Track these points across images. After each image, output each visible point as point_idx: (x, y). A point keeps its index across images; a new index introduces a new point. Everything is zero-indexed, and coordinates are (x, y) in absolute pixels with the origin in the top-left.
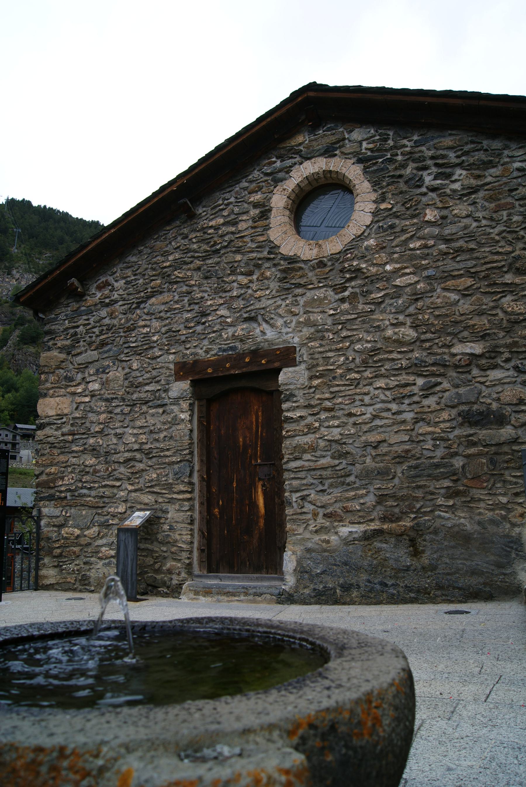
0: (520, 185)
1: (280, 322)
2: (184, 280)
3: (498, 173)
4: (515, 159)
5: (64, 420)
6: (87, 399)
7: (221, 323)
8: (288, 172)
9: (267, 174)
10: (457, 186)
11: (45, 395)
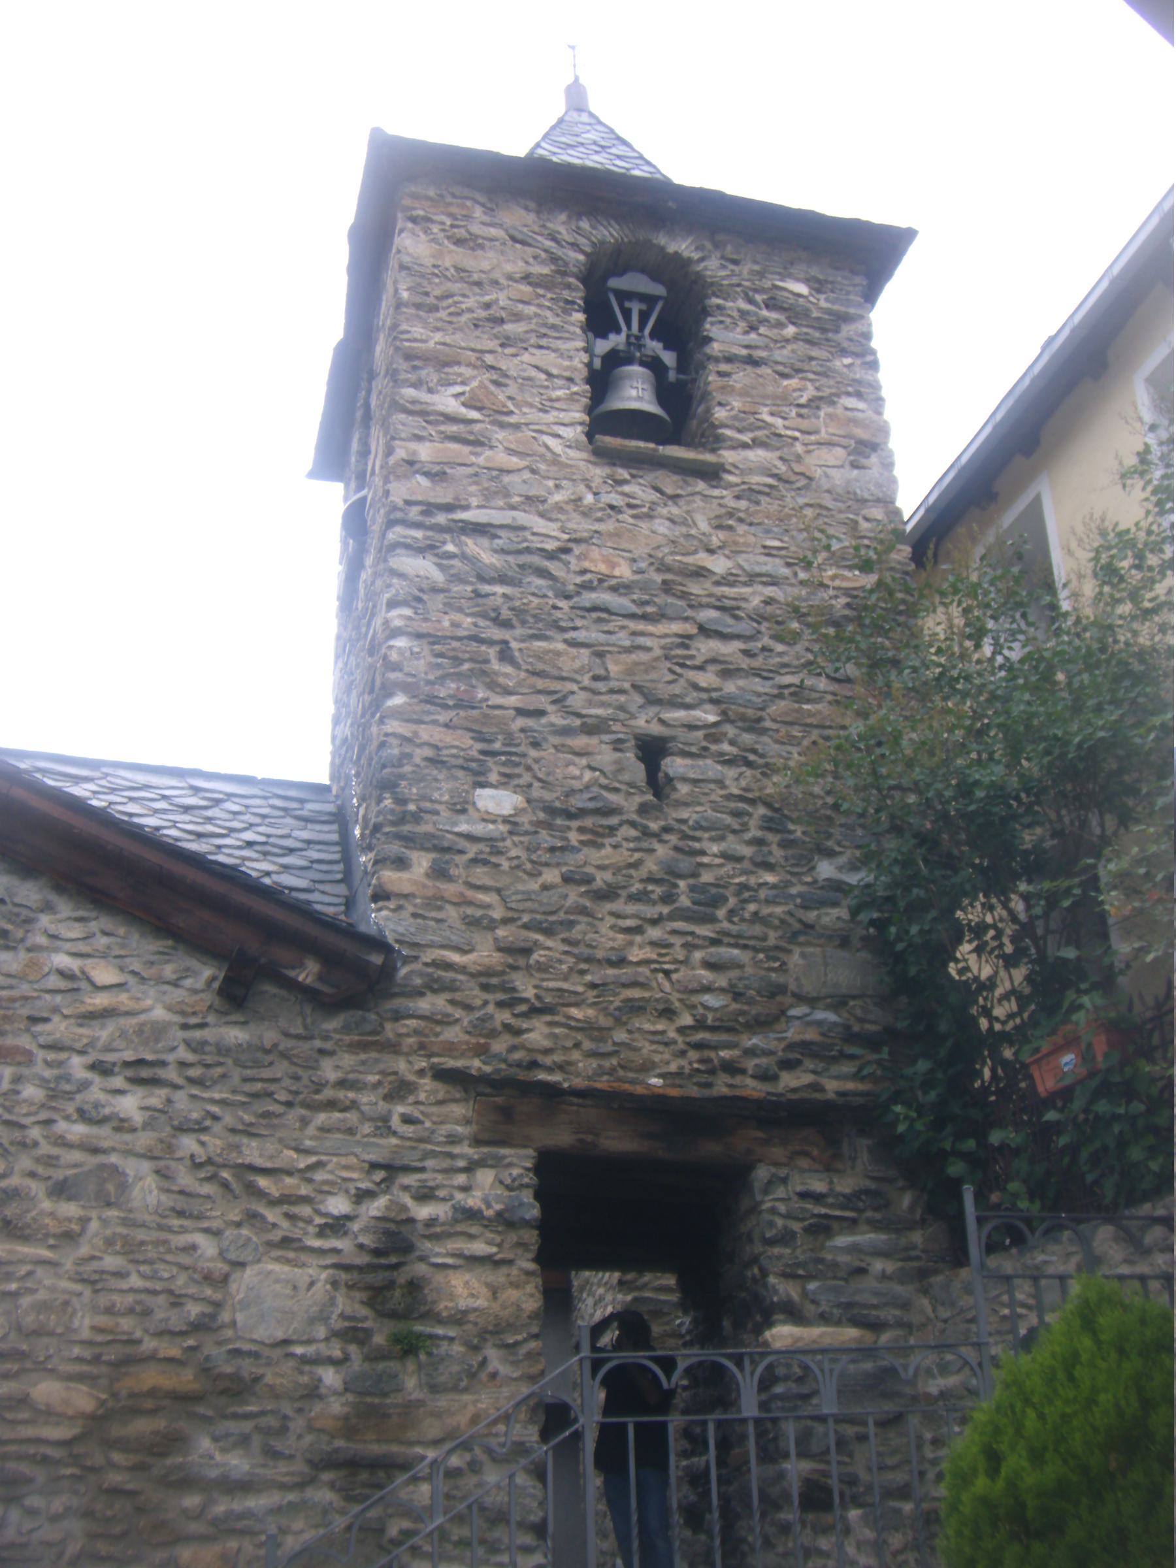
0: (56, 1010)
3: (14, 968)
4: (59, 943)
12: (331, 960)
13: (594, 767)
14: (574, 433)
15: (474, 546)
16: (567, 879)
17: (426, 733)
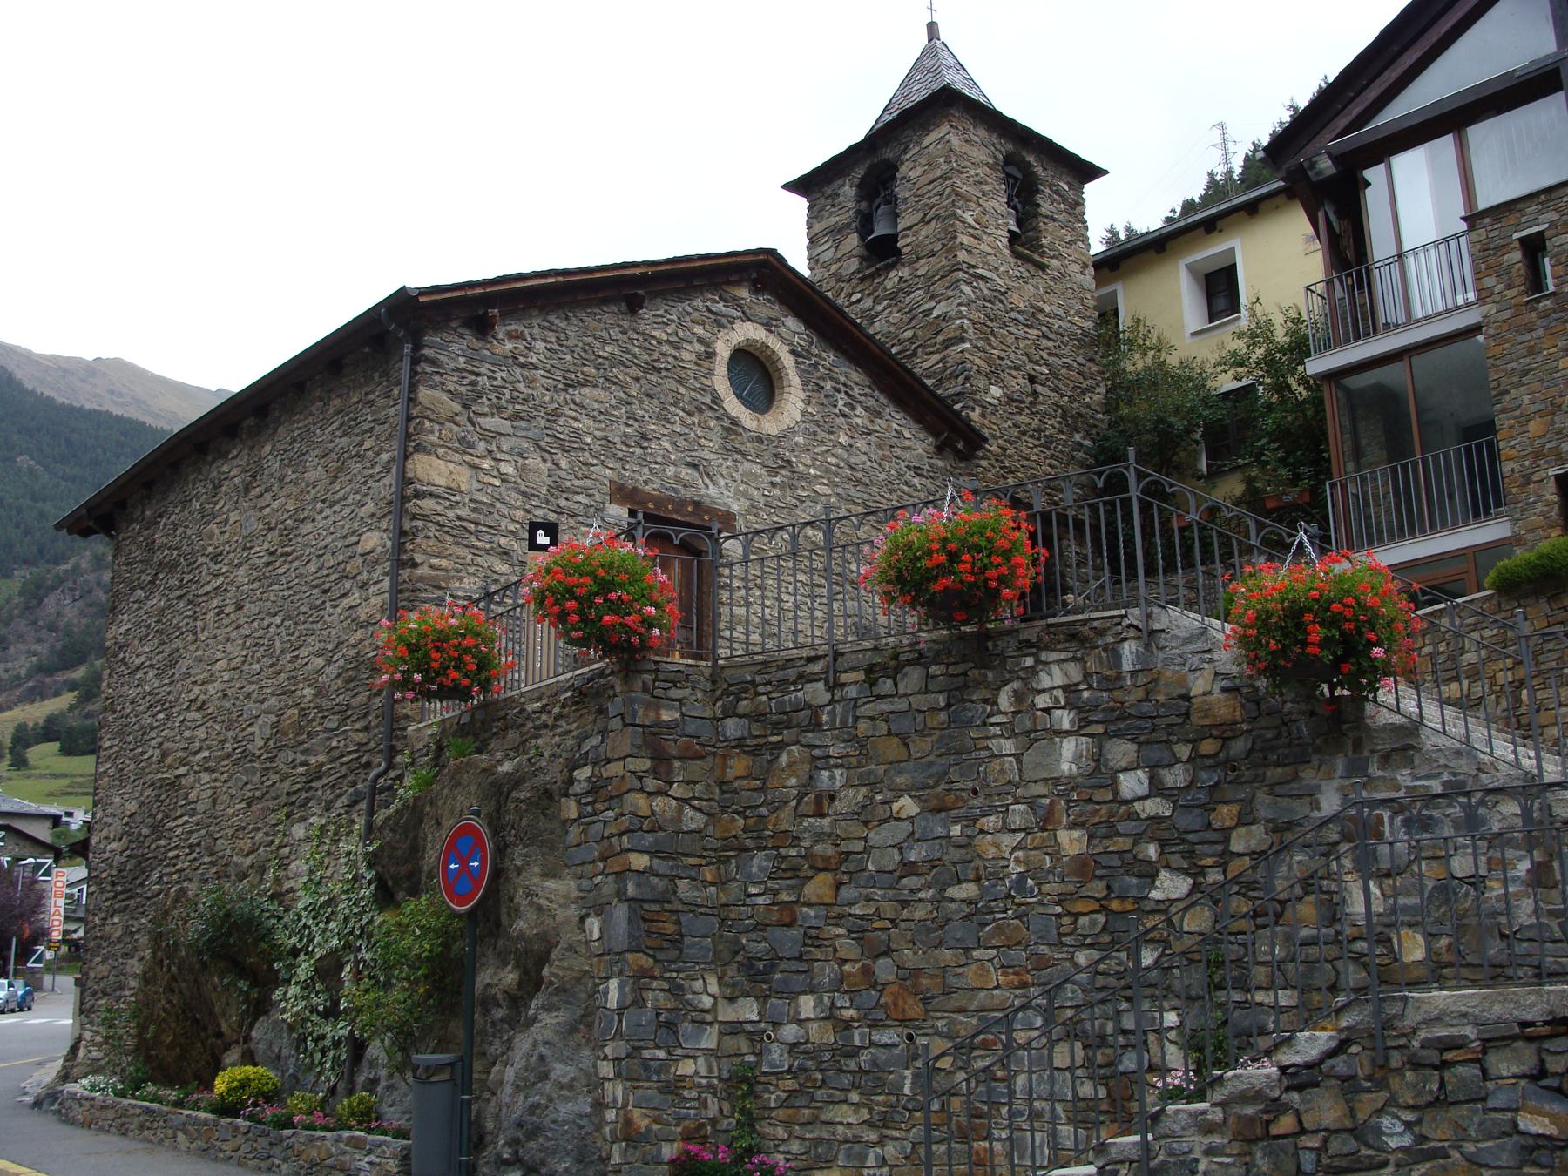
1: (722, 482)
2: (622, 385)
5: (458, 498)
6: (497, 482)
7: (663, 456)
8: (731, 323)
9: (709, 311)
10: (859, 421)
11: (429, 453)
12: (966, 439)
13: (1018, 383)
14: (1005, 241)
15: (982, 284)
16: (1015, 425)
17: (977, 361)
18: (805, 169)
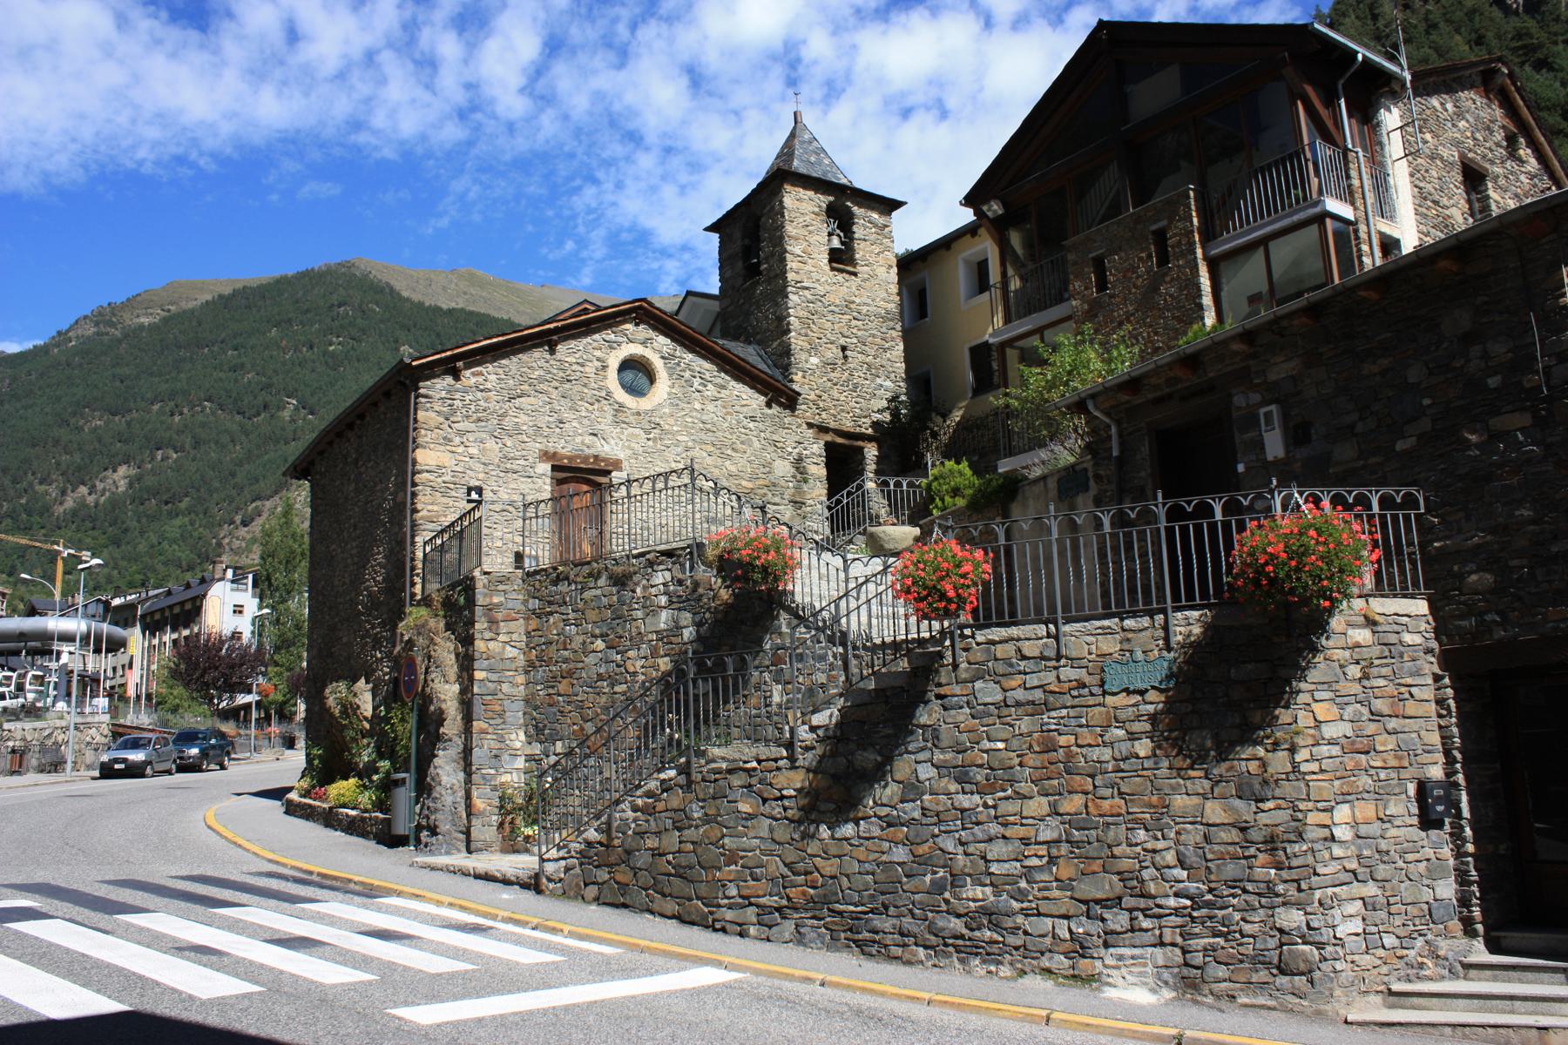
13: (833, 353)
18: (709, 223)
